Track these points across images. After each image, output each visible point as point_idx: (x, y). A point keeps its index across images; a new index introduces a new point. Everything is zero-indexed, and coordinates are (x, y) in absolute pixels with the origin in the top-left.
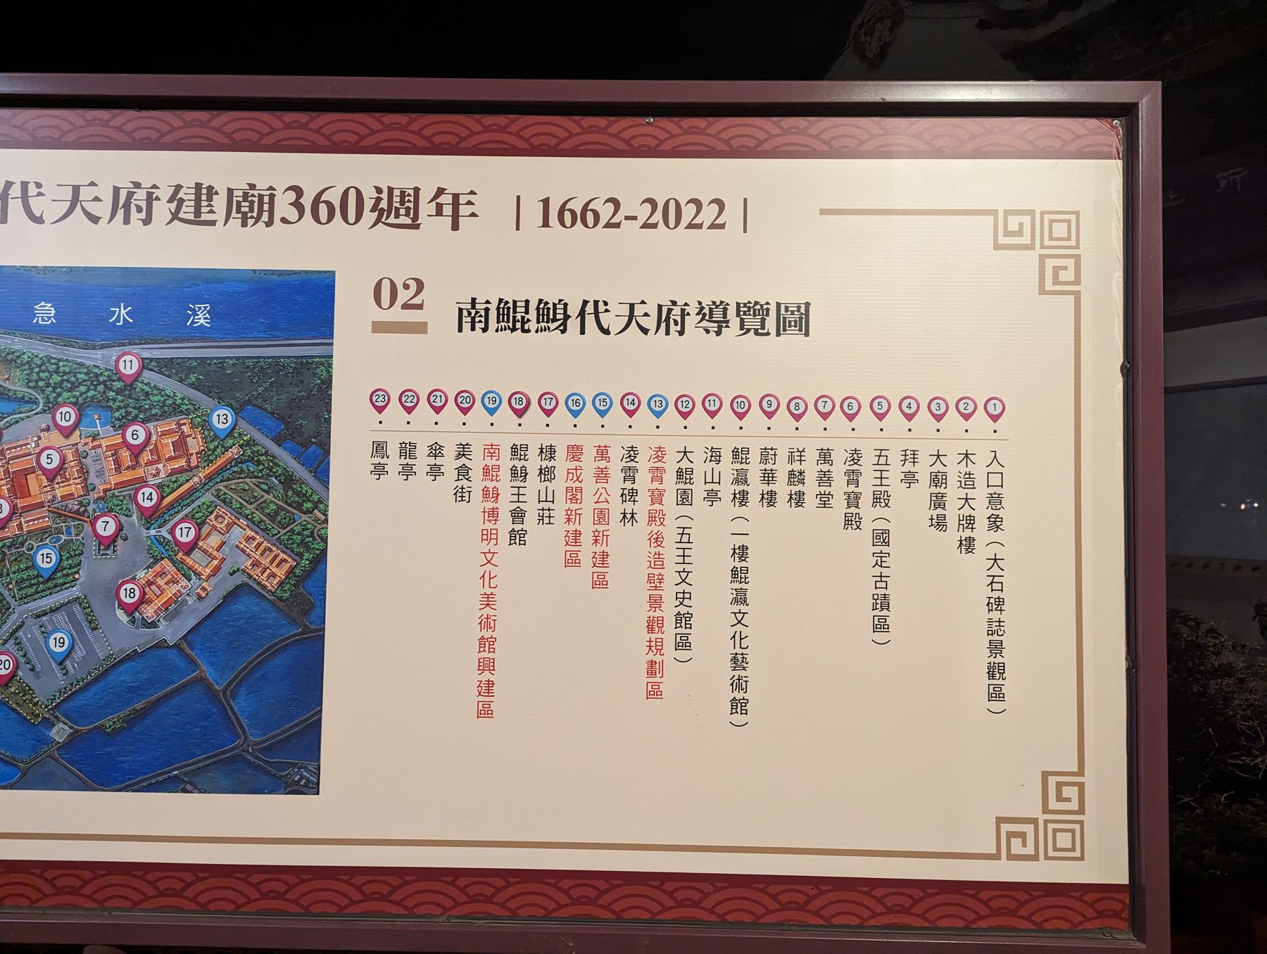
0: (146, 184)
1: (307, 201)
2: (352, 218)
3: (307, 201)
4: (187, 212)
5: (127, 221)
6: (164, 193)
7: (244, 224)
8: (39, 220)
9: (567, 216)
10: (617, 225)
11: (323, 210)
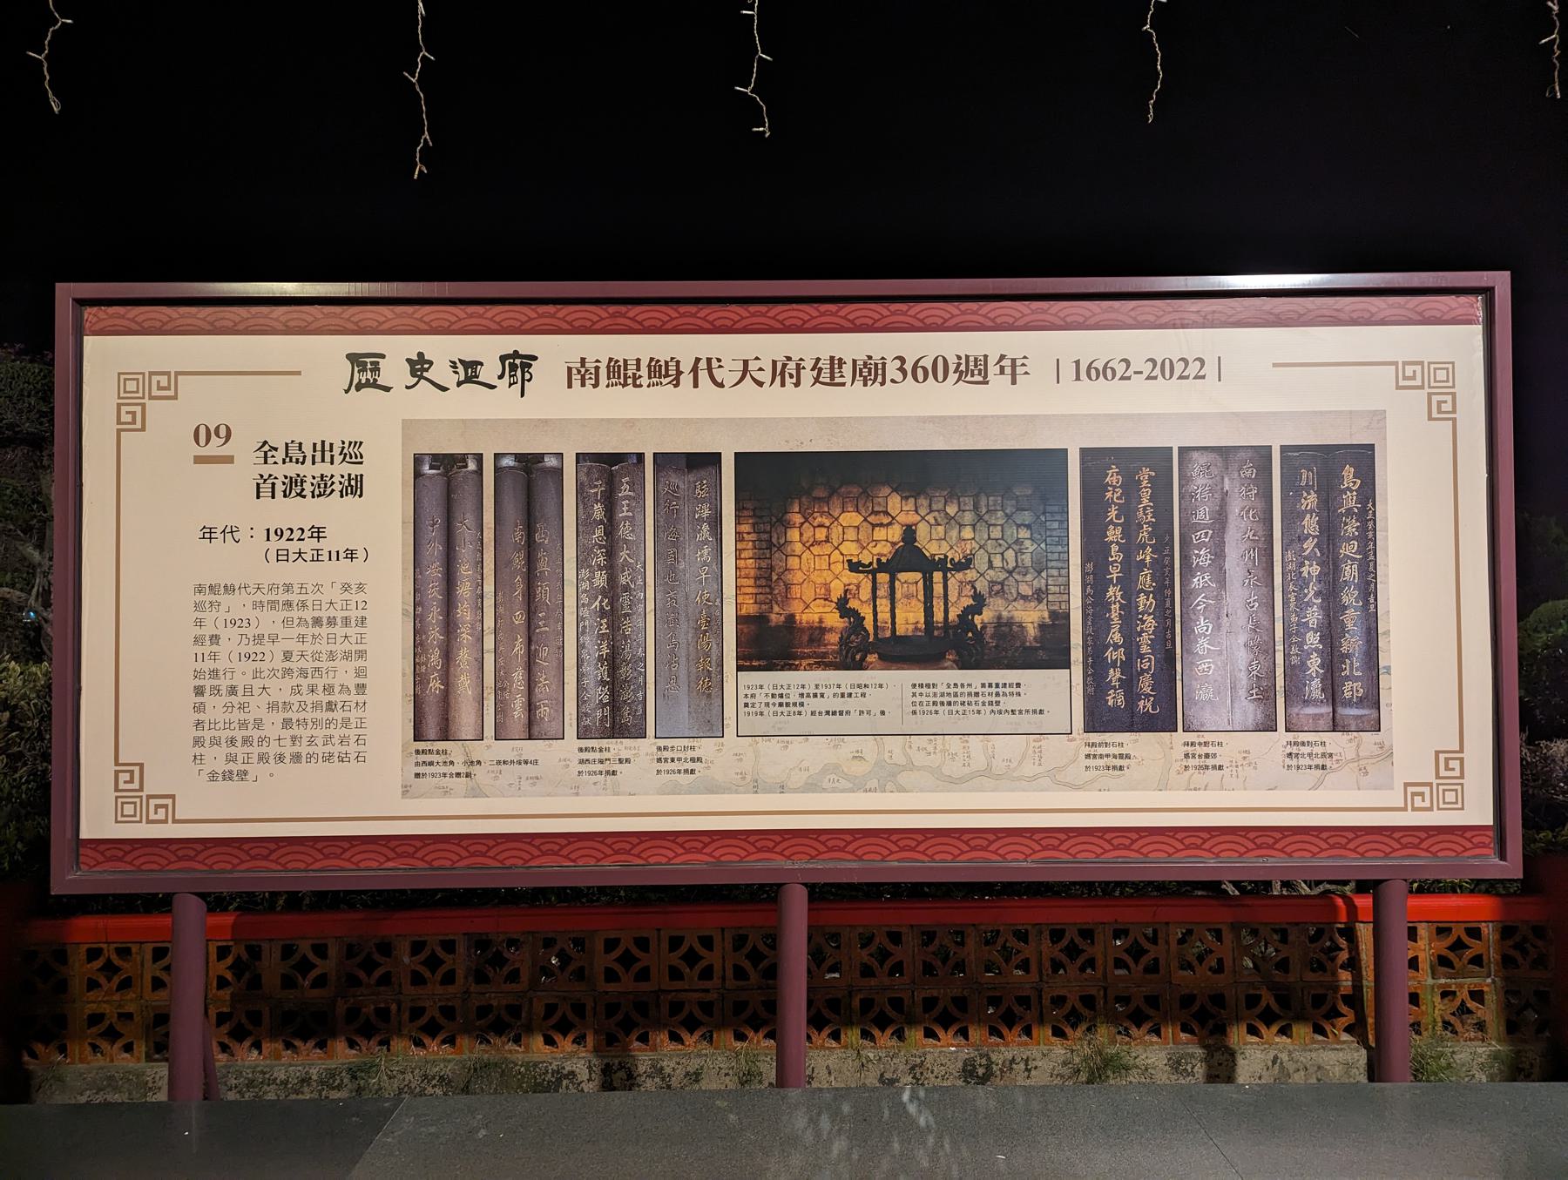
0: (795, 358)
1: (908, 367)
2: (940, 377)
3: (908, 367)
4: (825, 377)
5: (783, 385)
6: (808, 364)
7: (865, 385)
8: (721, 385)
9: (1093, 372)
10: (1129, 378)
11: (920, 372)
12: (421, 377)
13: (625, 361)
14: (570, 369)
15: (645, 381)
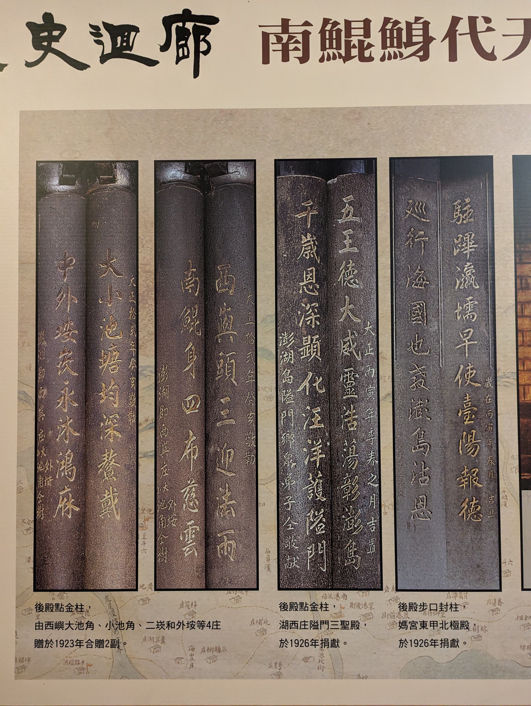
12: (49, 50)
13: (348, 23)
14: (265, 36)
15: (377, 52)
